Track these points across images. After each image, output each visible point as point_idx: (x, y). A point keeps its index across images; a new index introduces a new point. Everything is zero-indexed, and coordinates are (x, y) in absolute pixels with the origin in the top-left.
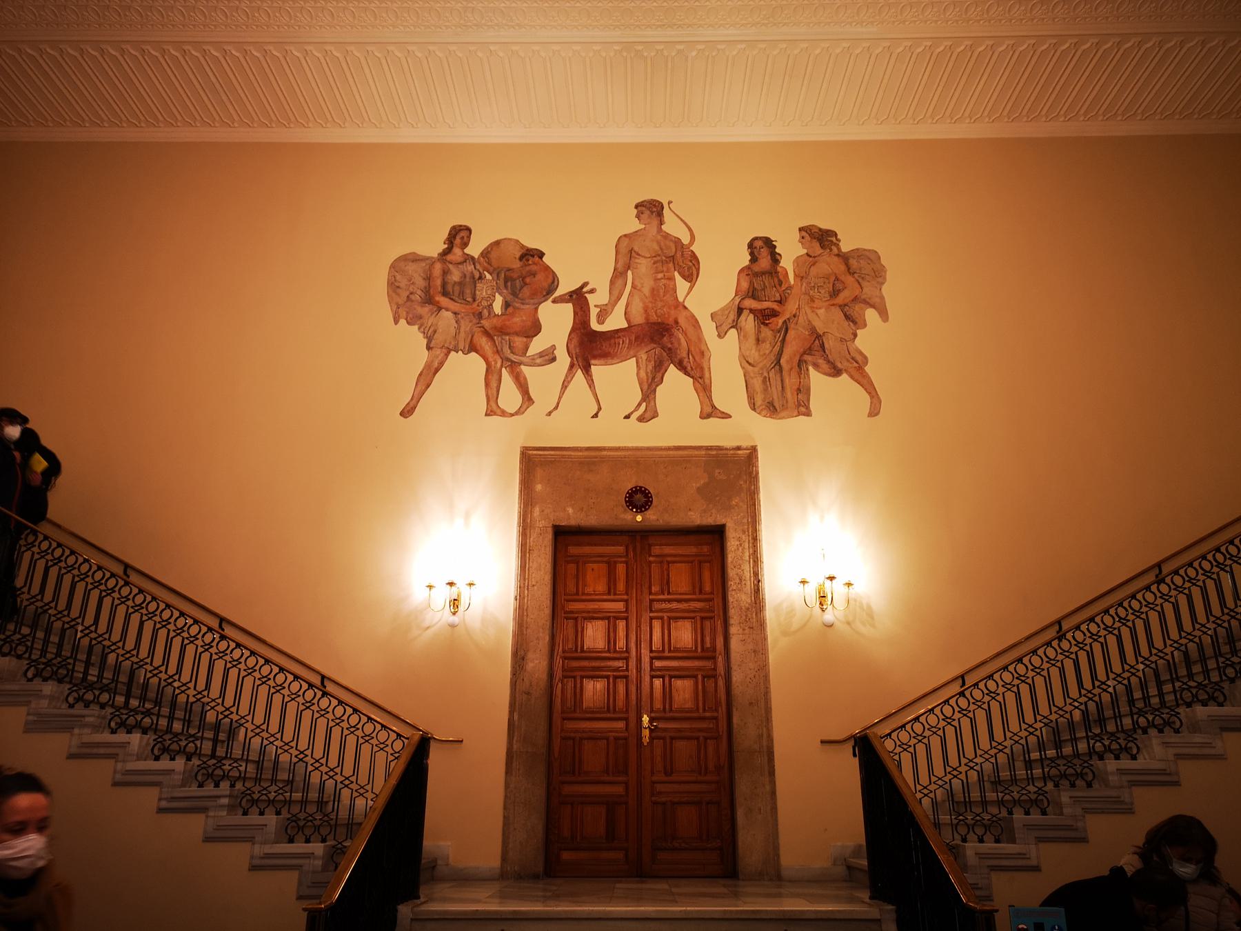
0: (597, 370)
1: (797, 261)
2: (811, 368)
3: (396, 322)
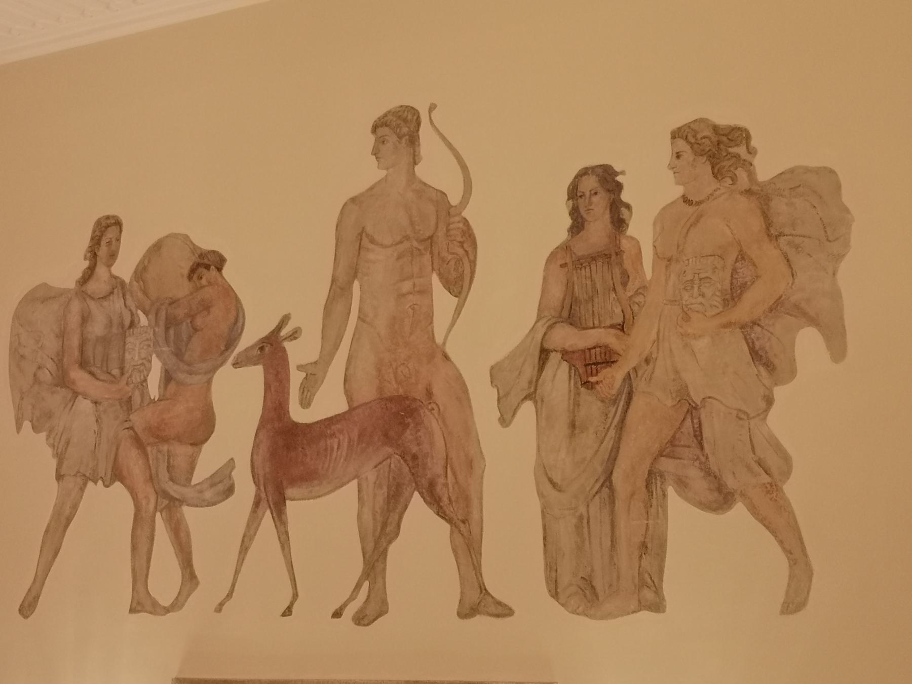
0: (296, 509)
1: (664, 219)
2: (671, 491)
3: (19, 428)
